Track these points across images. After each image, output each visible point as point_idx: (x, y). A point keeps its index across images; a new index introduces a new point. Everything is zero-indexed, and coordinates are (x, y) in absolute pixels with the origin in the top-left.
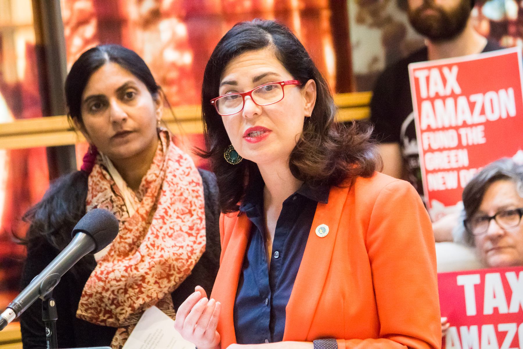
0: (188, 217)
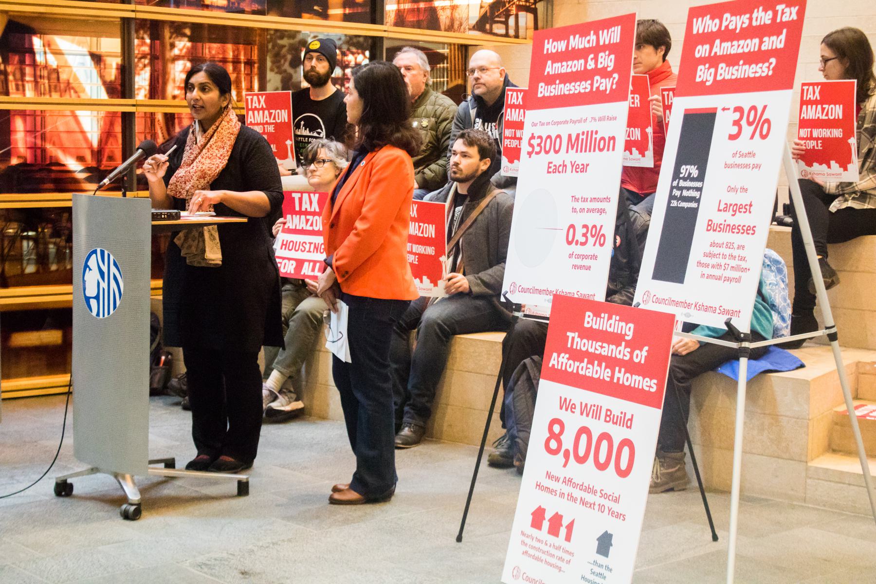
0: (222, 150)
